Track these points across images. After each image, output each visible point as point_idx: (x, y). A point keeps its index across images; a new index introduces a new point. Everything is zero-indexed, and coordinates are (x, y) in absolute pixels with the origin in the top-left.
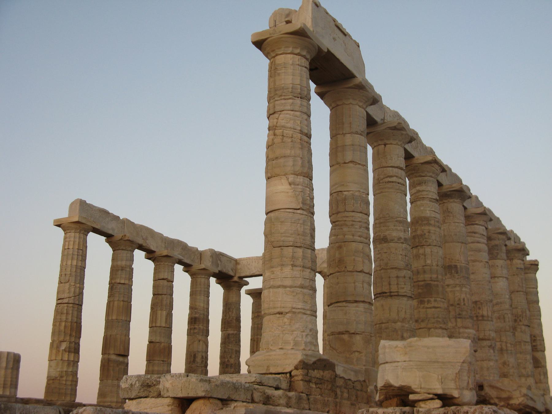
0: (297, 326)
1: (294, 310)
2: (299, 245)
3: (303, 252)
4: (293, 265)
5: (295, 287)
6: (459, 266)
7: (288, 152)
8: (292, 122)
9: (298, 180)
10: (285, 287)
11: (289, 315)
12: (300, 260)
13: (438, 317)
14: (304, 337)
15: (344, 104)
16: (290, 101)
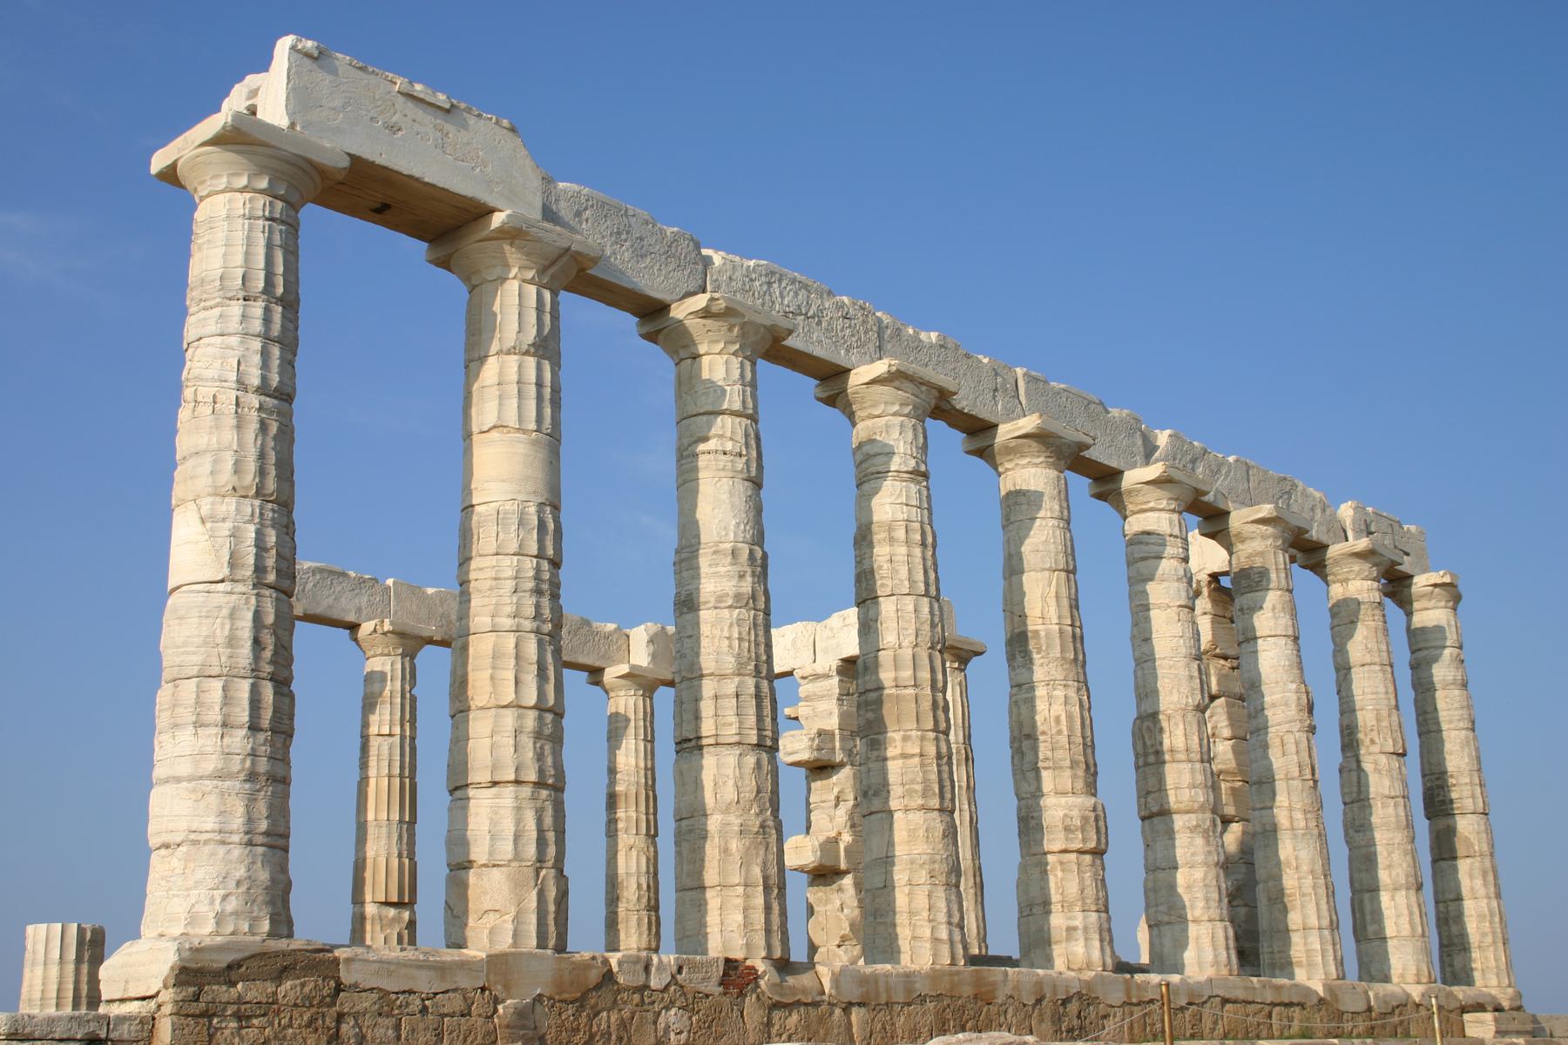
0: (200, 874)
1: (193, 836)
2: (215, 671)
3: (224, 689)
4: (198, 724)
5: (201, 778)
6: (1043, 634)
7: (203, 440)
8: (217, 364)
9: (224, 508)
10: (178, 780)
11: (183, 849)
12: (217, 708)
13: (913, 782)
14: (218, 902)
15: (485, 281)
16: (217, 311)
